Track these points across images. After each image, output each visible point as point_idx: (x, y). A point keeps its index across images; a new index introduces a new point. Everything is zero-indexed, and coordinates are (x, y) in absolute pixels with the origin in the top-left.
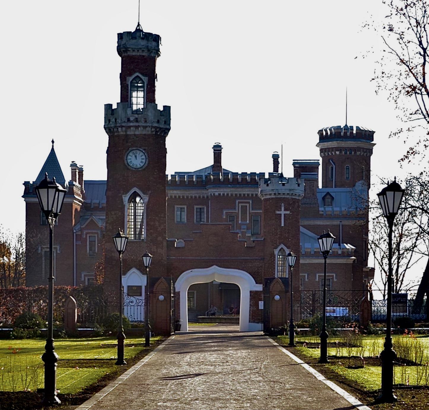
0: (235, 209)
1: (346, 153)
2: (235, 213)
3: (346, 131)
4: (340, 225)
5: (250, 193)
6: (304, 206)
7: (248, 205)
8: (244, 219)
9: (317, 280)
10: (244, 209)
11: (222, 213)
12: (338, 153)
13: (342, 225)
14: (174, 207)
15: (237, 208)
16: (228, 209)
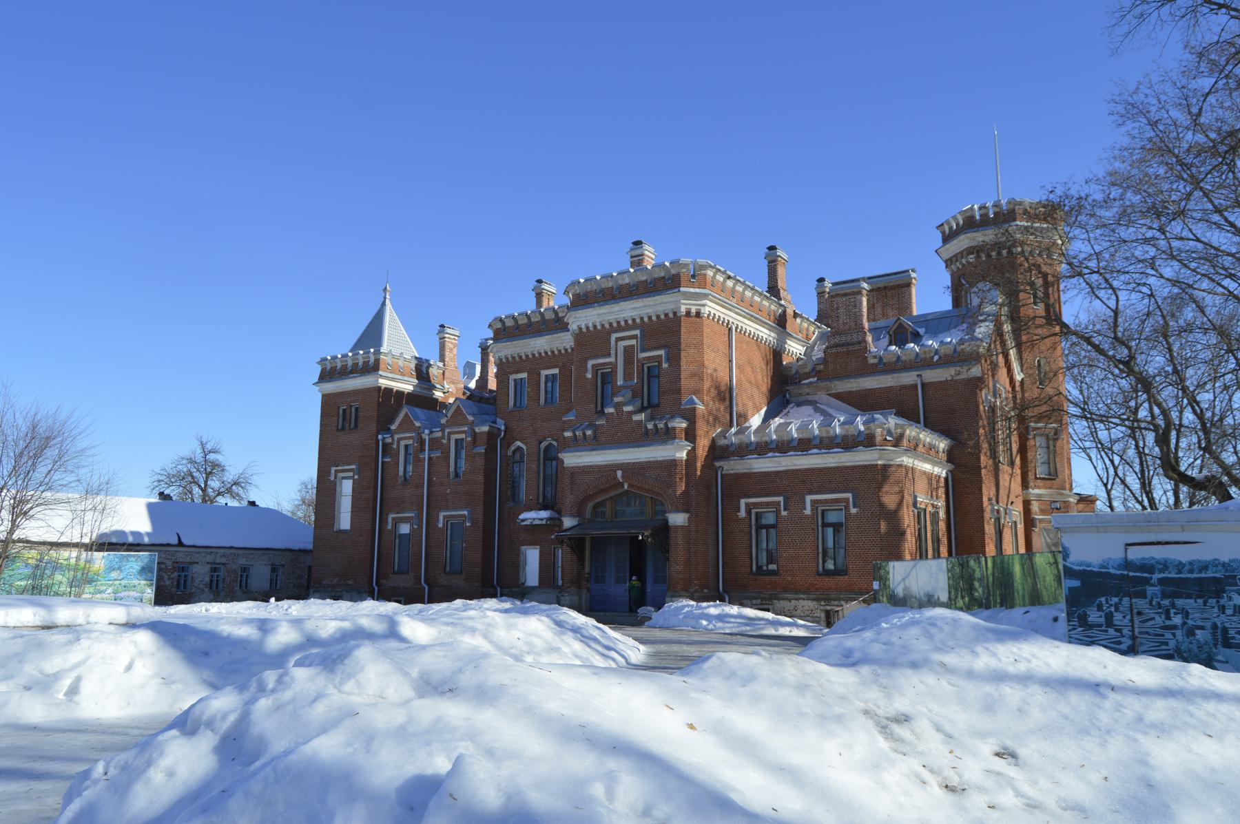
0: (609, 355)
1: (989, 256)
2: (610, 363)
3: (983, 211)
4: (916, 386)
5: (635, 314)
6: (834, 350)
7: (633, 342)
8: (628, 376)
9: (808, 511)
10: (628, 351)
11: (586, 370)
12: (971, 258)
13: (923, 385)
14: (539, 374)
15: (613, 352)
16: (596, 357)
